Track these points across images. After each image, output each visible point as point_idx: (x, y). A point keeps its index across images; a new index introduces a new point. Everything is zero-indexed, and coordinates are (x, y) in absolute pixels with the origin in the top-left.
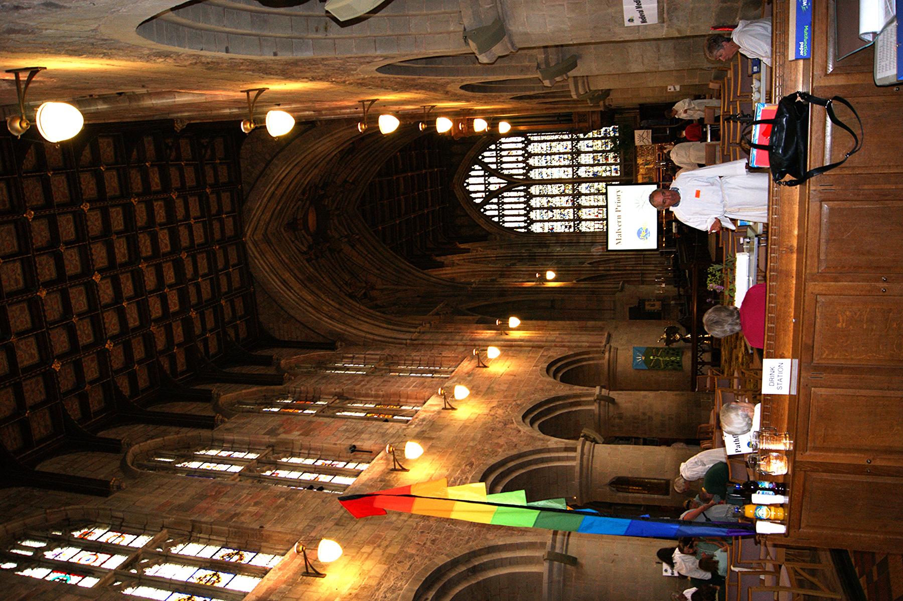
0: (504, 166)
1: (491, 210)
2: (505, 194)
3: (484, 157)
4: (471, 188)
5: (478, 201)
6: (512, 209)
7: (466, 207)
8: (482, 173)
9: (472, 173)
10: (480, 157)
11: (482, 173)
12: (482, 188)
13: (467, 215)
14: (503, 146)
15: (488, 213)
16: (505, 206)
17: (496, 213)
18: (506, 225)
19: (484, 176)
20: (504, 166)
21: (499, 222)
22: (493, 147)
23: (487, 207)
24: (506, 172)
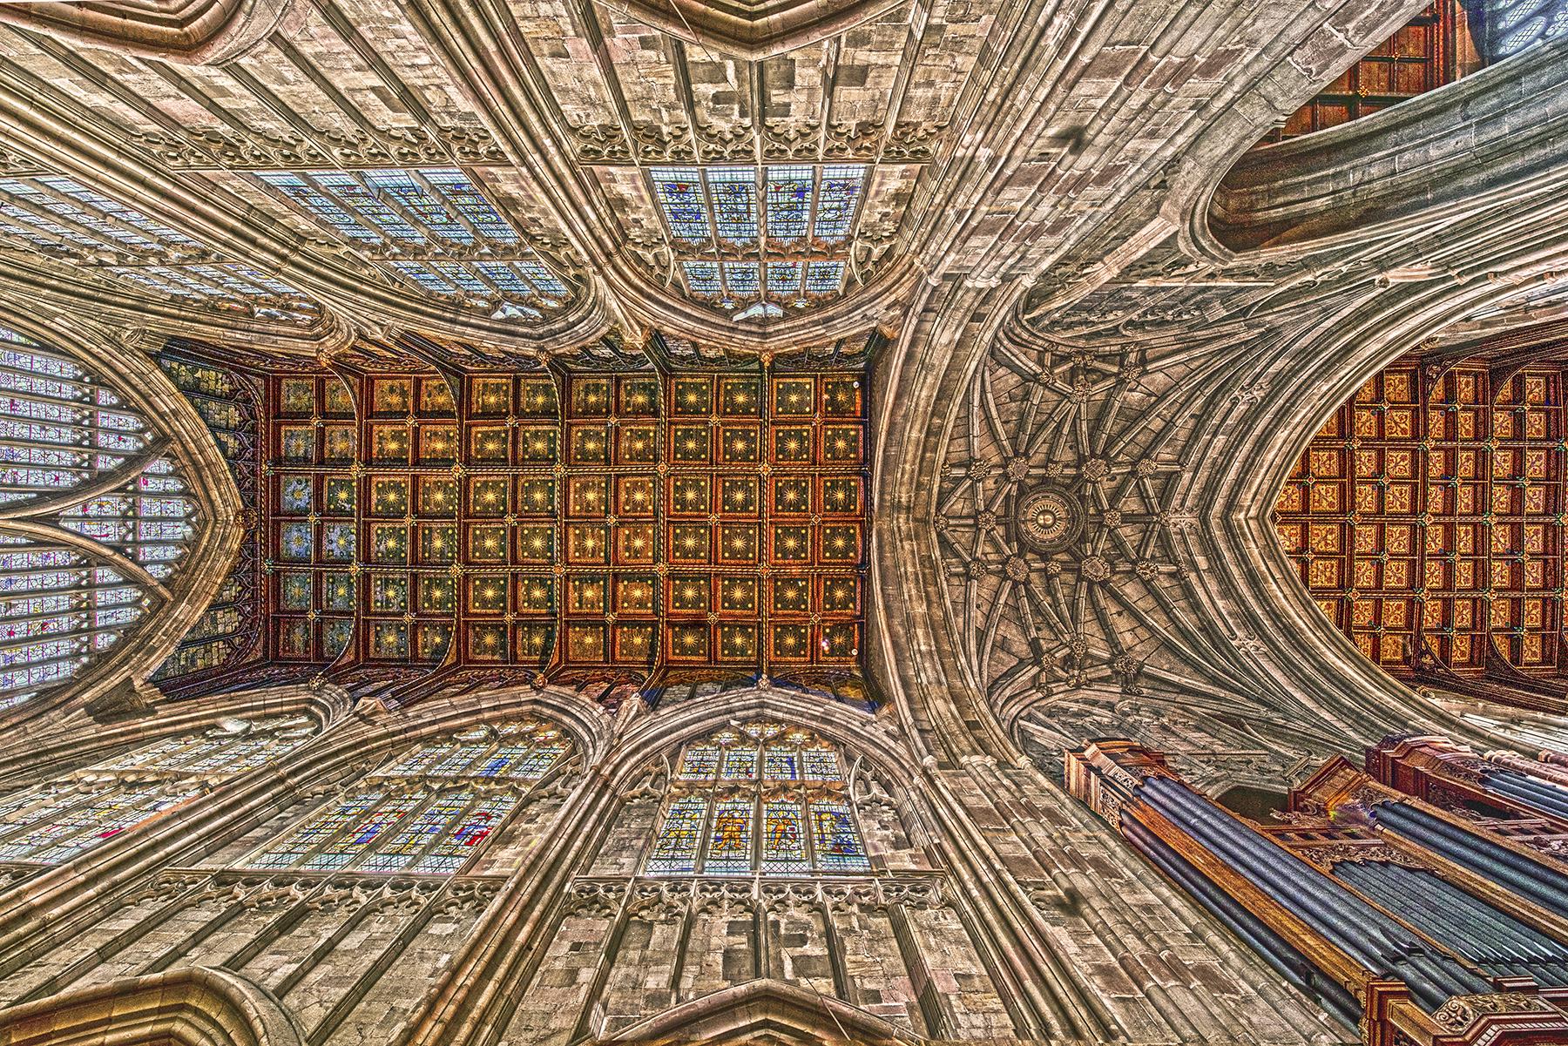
0: (67, 579)
1: (120, 434)
2: (67, 481)
3: (136, 603)
4: (179, 507)
5: (161, 465)
6: (44, 423)
7: (214, 453)
8: (147, 553)
9: (172, 553)
10: (147, 602)
11: (147, 553)
12: (149, 507)
13: (214, 428)
14: (66, 646)
15: (131, 422)
16: (68, 435)
17: (106, 420)
18: (69, 369)
19: (136, 543)
20: (67, 579)
21: (98, 382)
22: (103, 641)
23: (131, 445)
24: (60, 557)
